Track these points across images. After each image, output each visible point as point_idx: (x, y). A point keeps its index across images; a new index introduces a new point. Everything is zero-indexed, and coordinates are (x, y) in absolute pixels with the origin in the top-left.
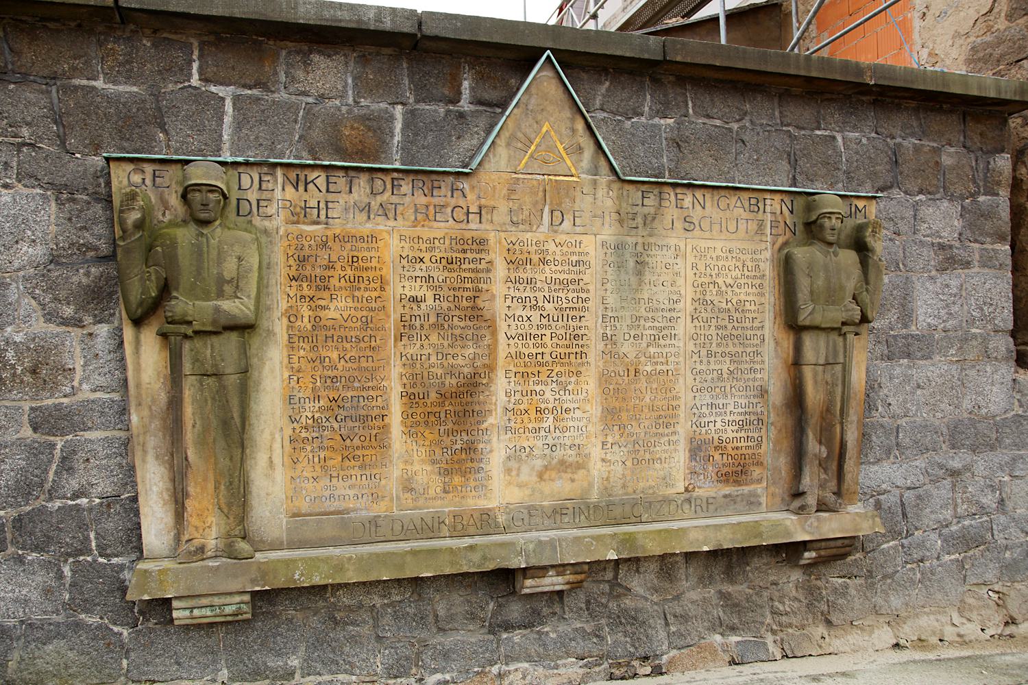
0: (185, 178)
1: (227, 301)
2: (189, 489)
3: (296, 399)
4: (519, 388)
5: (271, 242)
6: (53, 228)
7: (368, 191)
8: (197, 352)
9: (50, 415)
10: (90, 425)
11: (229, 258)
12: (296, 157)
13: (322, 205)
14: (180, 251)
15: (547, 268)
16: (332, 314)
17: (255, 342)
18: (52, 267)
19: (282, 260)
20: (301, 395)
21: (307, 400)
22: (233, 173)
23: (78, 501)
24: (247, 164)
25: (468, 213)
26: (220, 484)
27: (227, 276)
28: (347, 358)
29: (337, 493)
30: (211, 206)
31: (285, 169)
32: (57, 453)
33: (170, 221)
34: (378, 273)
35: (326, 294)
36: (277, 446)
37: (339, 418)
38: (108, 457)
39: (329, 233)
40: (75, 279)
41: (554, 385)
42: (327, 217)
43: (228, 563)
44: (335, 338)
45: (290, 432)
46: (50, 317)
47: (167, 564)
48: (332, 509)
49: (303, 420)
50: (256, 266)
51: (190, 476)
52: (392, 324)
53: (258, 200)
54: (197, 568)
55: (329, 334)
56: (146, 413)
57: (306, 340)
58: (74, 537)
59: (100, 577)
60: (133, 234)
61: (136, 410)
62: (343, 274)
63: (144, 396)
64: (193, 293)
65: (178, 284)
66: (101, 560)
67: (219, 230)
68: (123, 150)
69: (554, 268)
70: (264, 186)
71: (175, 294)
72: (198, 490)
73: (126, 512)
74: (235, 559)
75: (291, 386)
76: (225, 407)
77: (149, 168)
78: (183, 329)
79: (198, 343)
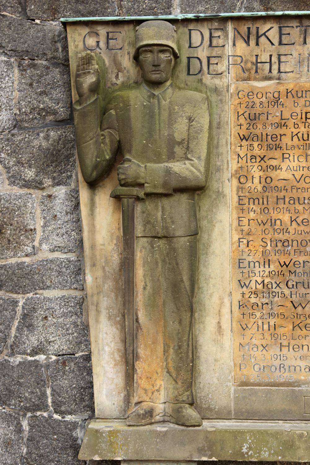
0: (137, 38)
1: (178, 164)
2: (139, 350)
3: (246, 263)
5: (221, 100)
6: (16, 94)
8: (149, 214)
9: (13, 273)
10: (48, 283)
11: (179, 120)
12: (248, 9)
13: (274, 59)
14: (132, 114)
16: (283, 174)
17: (205, 204)
18: (15, 131)
19: (233, 119)
20: (250, 259)
21: (257, 264)
22: (183, 30)
23: (37, 358)
24: (197, 20)
26: (169, 347)
27: (178, 137)
28: (299, 220)
30: (162, 66)
31: (236, 23)
32: (19, 309)
33: (123, 83)
35: (277, 154)
36: (226, 310)
37: (290, 284)
38: (64, 315)
39: (282, 89)
40: (36, 143)
42: (279, 71)
43: (175, 430)
44: (287, 200)
45: (239, 297)
46: (14, 179)
47: (117, 425)
48: (282, 380)
49: (253, 284)
50: (206, 127)
51: (140, 338)
53: (209, 58)
54: (145, 431)
55: (281, 195)
56: (100, 273)
57: (256, 201)
58: (32, 393)
59: (55, 434)
60: (89, 97)
61: (91, 271)
62: (295, 131)
63: (98, 257)
64: (144, 156)
65: (131, 146)
66: (56, 416)
67: (170, 91)
68: (78, 13)
70: (214, 43)
71: (127, 156)
72: (148, 352)
73: (80, 370)
74: (183, 425)
75: (240, 249)
76: (175, 270)
77: (102, 31)
78: (136, 191)
79: (149, 205)
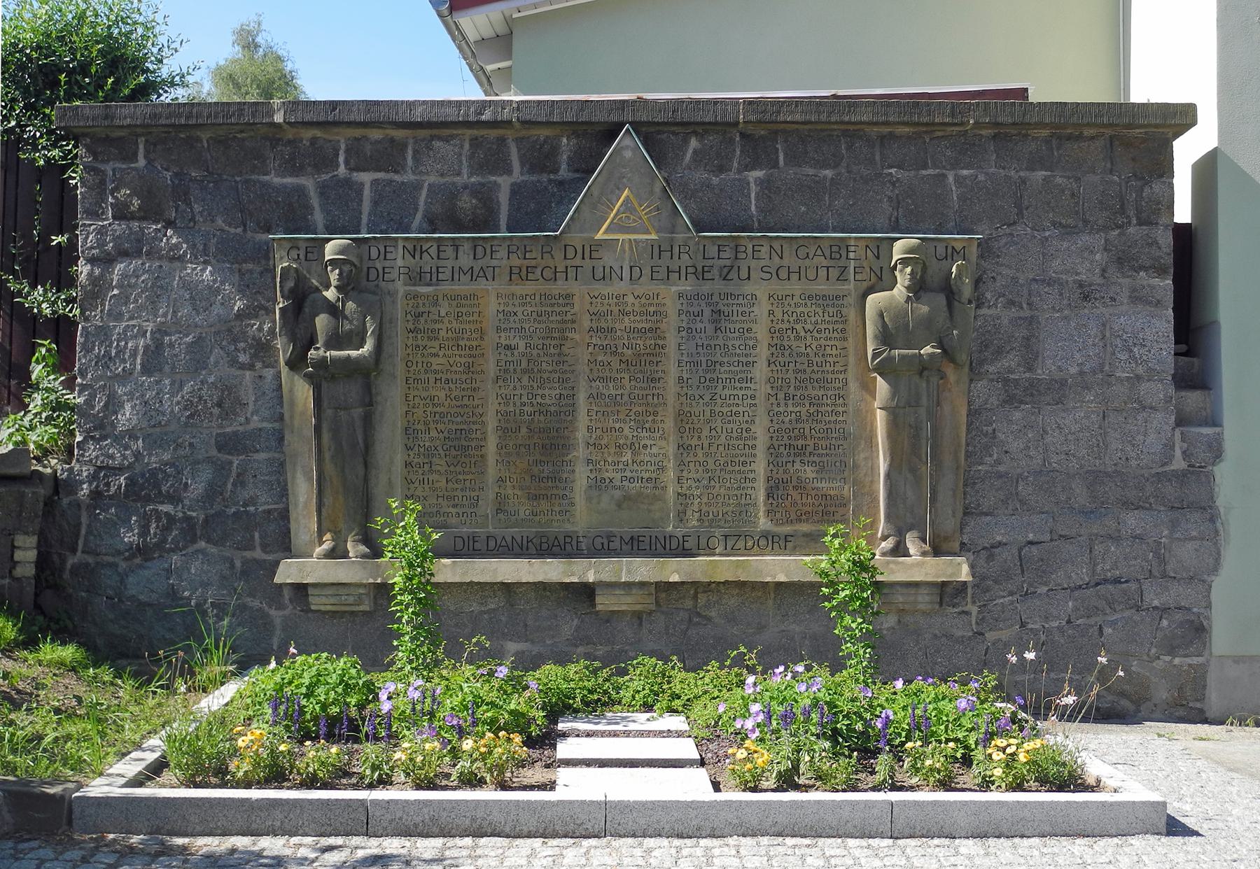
4: (599, 425)
7: (472, 257)
13: (434, 270)
15: (626, 319)
25: (556, 272)
28: (452, 397)
29: (442, 511)
34: (478, 326)
41: (632, 423)
46: (233, 362)
52: (491, 369)
69: (632, 318)
